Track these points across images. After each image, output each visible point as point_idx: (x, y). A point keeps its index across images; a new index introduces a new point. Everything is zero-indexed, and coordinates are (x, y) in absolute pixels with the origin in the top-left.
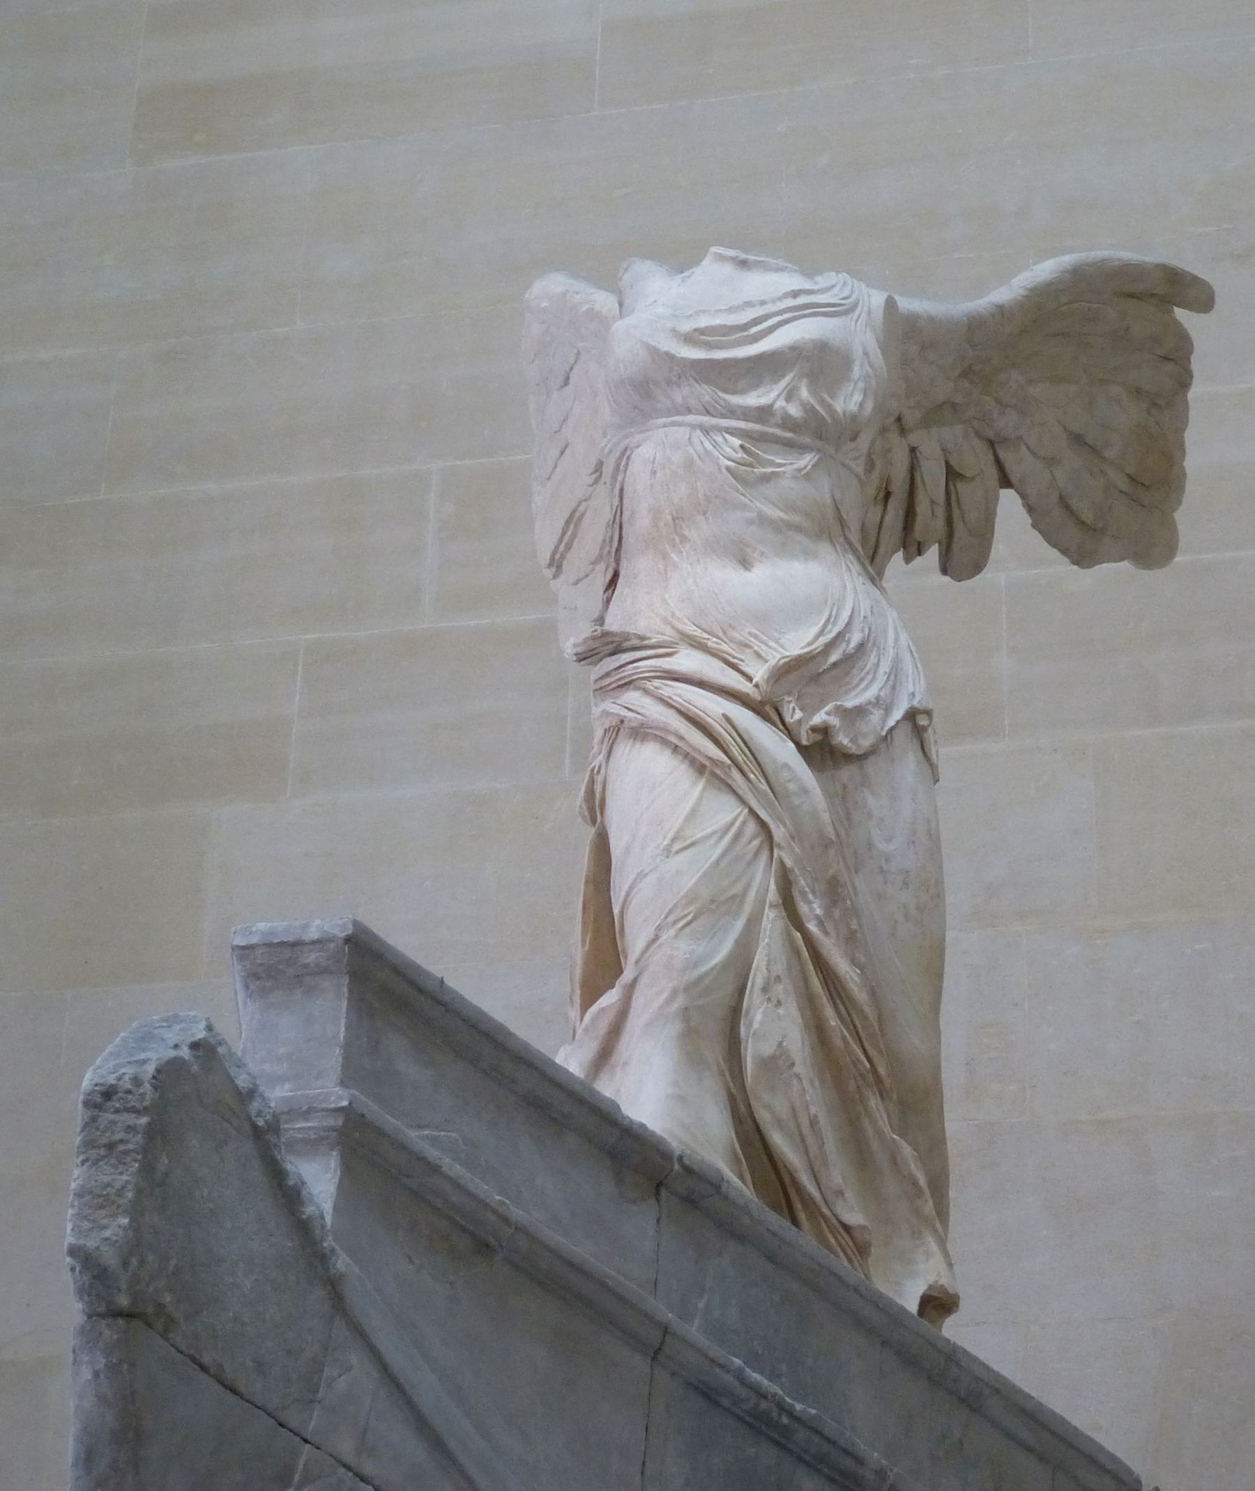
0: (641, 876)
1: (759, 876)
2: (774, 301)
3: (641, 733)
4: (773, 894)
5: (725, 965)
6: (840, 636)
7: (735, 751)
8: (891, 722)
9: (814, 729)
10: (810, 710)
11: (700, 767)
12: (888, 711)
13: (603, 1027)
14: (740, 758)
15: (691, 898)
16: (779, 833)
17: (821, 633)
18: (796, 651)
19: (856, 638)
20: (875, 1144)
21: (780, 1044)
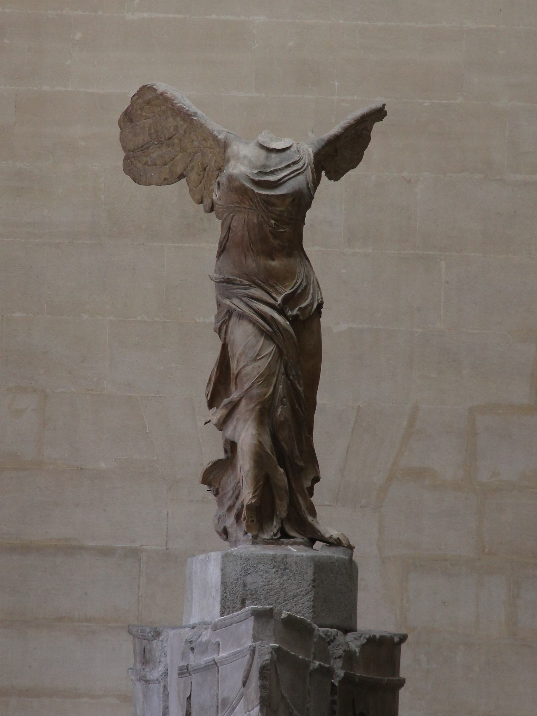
0: (247, 365)
1: (279, 364)
2: (282, 170)
3: (242, 316)
4: (283, 370)
7: (274, 327)
8: (313, 310)
9: (294, 316)
11: (262, 332)
12: (313, 306)
13: (230, 407)
14: (276, 329)
15: (262, 375)
16: (285, 351)
18: (288, 291)
19: (304, 284)
20: (303, 437)
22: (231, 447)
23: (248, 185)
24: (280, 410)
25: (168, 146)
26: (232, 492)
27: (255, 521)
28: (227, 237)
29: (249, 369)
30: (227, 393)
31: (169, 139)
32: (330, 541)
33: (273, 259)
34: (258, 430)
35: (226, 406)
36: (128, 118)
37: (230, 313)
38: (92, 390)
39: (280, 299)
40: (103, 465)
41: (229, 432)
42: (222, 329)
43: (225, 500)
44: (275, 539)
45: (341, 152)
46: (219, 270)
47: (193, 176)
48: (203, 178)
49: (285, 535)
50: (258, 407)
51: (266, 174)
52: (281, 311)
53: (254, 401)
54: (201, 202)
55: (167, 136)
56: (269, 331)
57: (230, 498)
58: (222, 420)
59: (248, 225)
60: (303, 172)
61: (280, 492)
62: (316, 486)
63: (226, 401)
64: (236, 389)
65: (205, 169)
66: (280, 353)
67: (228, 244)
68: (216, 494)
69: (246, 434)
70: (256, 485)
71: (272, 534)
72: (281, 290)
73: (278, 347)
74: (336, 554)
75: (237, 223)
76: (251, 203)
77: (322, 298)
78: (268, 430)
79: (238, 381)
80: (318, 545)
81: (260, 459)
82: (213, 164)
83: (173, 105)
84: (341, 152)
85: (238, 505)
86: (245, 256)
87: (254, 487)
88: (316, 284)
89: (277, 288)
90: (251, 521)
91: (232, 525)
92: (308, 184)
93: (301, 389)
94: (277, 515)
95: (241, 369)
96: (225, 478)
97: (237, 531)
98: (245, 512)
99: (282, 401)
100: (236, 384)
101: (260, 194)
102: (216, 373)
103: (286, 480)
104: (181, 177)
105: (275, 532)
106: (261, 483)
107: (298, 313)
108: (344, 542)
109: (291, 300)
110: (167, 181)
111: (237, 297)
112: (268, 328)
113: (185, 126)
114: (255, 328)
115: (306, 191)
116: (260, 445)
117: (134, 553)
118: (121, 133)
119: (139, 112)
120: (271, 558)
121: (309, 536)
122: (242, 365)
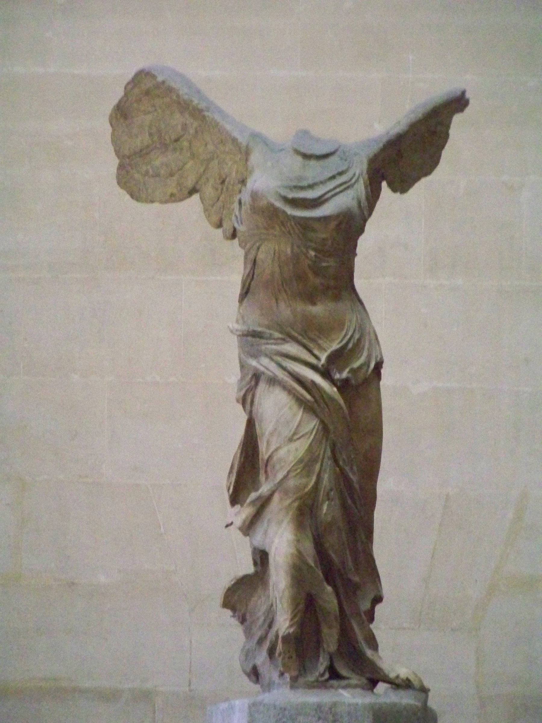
1: (323, 446)
3: (273, 381)
4: (329, 453)
5: (313, 487)
6: (352, 336)
7: (317, 396)
10: (340, 372)
11: (300, 401)
12: (369, 366)
13: (258, 504)
15: (301, 461)
16: (331, 427)
17: (345, 336)
18: (335, 346)
21: (333, 516)
22: (262, 558)
23: (279, 204)
24: (325, 507)
25: (175, 150)
26: (263, 618)
27: (294, 656)
28: (251, 275)
29: (282, 452)
30: (256, 486)
31: (177, 140)
32: (397, 682)
33: (314, 304)
34: (296, 535)
35: (253, 502)
36: (122, 113)
37: (257, 377)
38: (86, 477)
39: (323, 358)
40: (103, 579)
41: (258, 539)
42: (247, 400)
43: (255, 630)
44: (322, 682)
45: (409, 154)
46: (242, 318)
47: (209, 190)
48: (222, 193)
49: (334, 674)
50: (296, 504)
51: (302, 188)
52: (326, 374)
53: (291, 495)
54: (219, 225)
55: (173, 137)
57: (259, 626)
58: (247, 523)
59: (279, 258)
60: (352, 186)
62: (378, 608)
63: (253, 495)
64: (267, 478)
65: (223, 182)
67: (252, 283)
68: (243, 620)
69: (282, 540)
70: (295, 609)
71: (317, 674)
72: (325, 345)
73: (322, 422)
74: (406, 699)
76: (283, 229)
77: (381, 355)
78: (310, 535)
79: (269, 469)
80: (381, 687)
81: (299, 573)
82: (234, 174)
83: (178, 96)
84: (409, 154)
85: (271, 636)
86: (277, 300)
87: (293, 612)
88: (372, 335)
89: (320, 342)
90: (289, 658)
91: (264, 663)
92: (359, 202)
93: (354, 478)
94: (324, 649)
95: (272, 453)
96: (254, 599)
97: (270, 672)
98: (280, 647)
99: (328, 494)
100: (266, 472)
101: (294, 217)
102: (241, 458)
103: (335, 601)
104: (192, 191)
105: (322, 672)
106: (302, 606)
107: (350, 375)
108: (416, 683)
110: (173, 198)
111: (266, 355)
112: (308, 397)
113: (195, 124)
114: (290, 397)
115: (356, 210)
116: (300, 555)
117: (145, 696)
118: (113, 134)
119: (135, 105)
120: (315, 707)
121: (368, 675)
122: (272, 448)
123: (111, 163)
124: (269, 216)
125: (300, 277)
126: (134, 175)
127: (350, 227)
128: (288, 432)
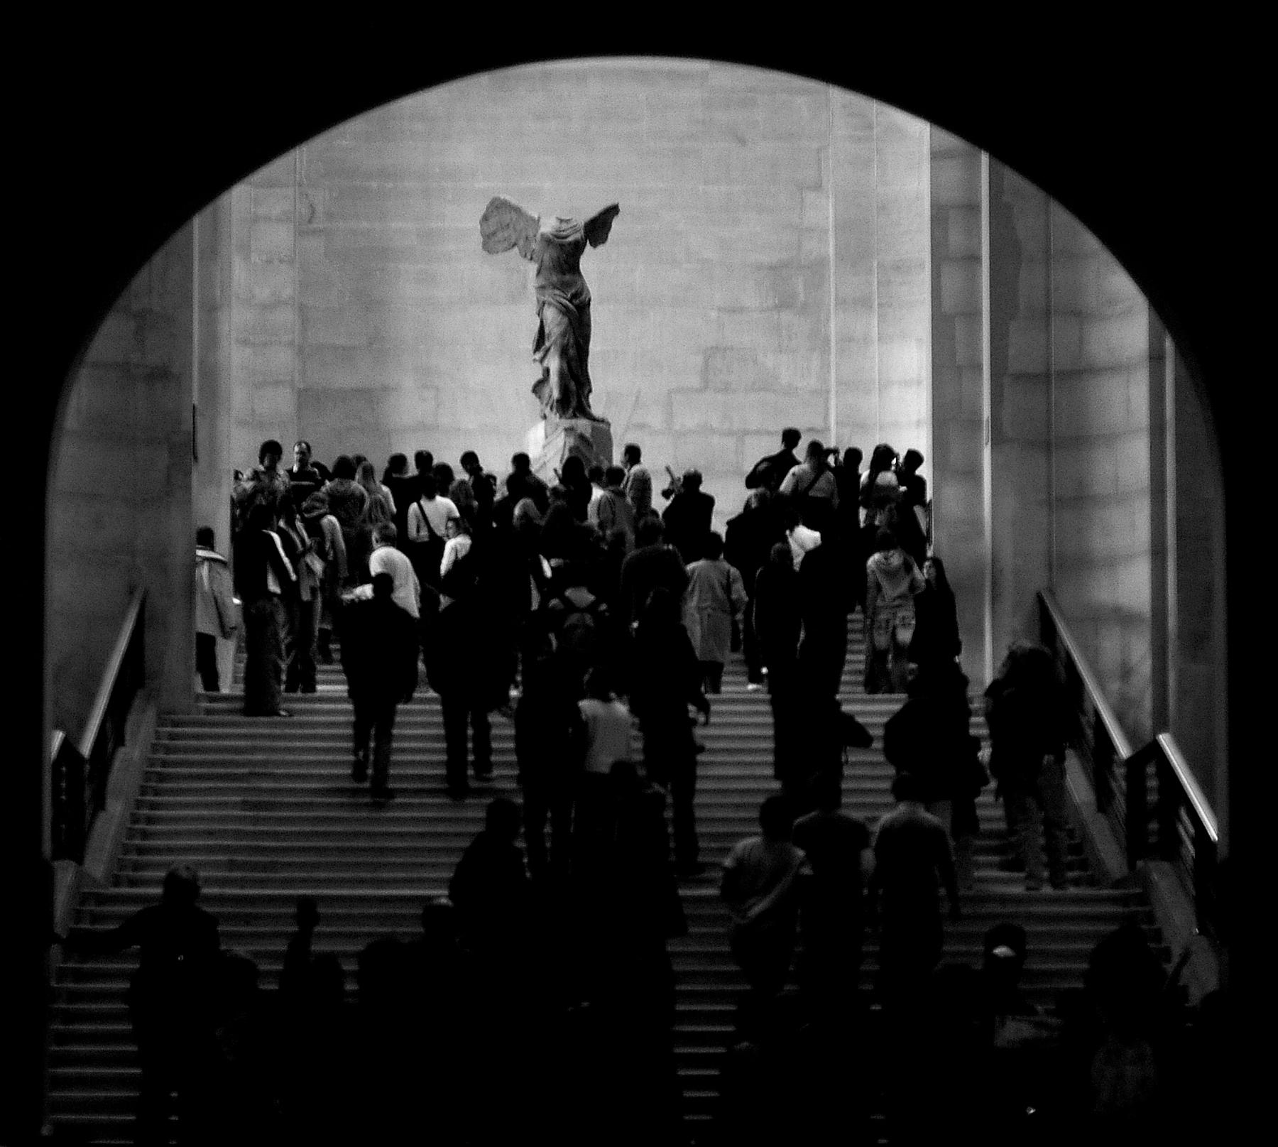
3: (550, 304)
22: (547, 371)
36: (485, 218)
41: (545, 364)
42: (540, 313)
45: (598, 229)
47: (521, 242)
49: (575, 416)
52: (570, 301)
56: (565, 311)
61: (573, 394)
66: (570, 323)
69: (554, 363)
75: (546, 257)
81: (562, 376)
84: (598, 229)
109: (575, 296)
110: (506, 250)
123: (478, 239)
124: (548, 241)
125: (560, 266)
126: (490, 243)
127: (578, 248)
128: (554, 321)
